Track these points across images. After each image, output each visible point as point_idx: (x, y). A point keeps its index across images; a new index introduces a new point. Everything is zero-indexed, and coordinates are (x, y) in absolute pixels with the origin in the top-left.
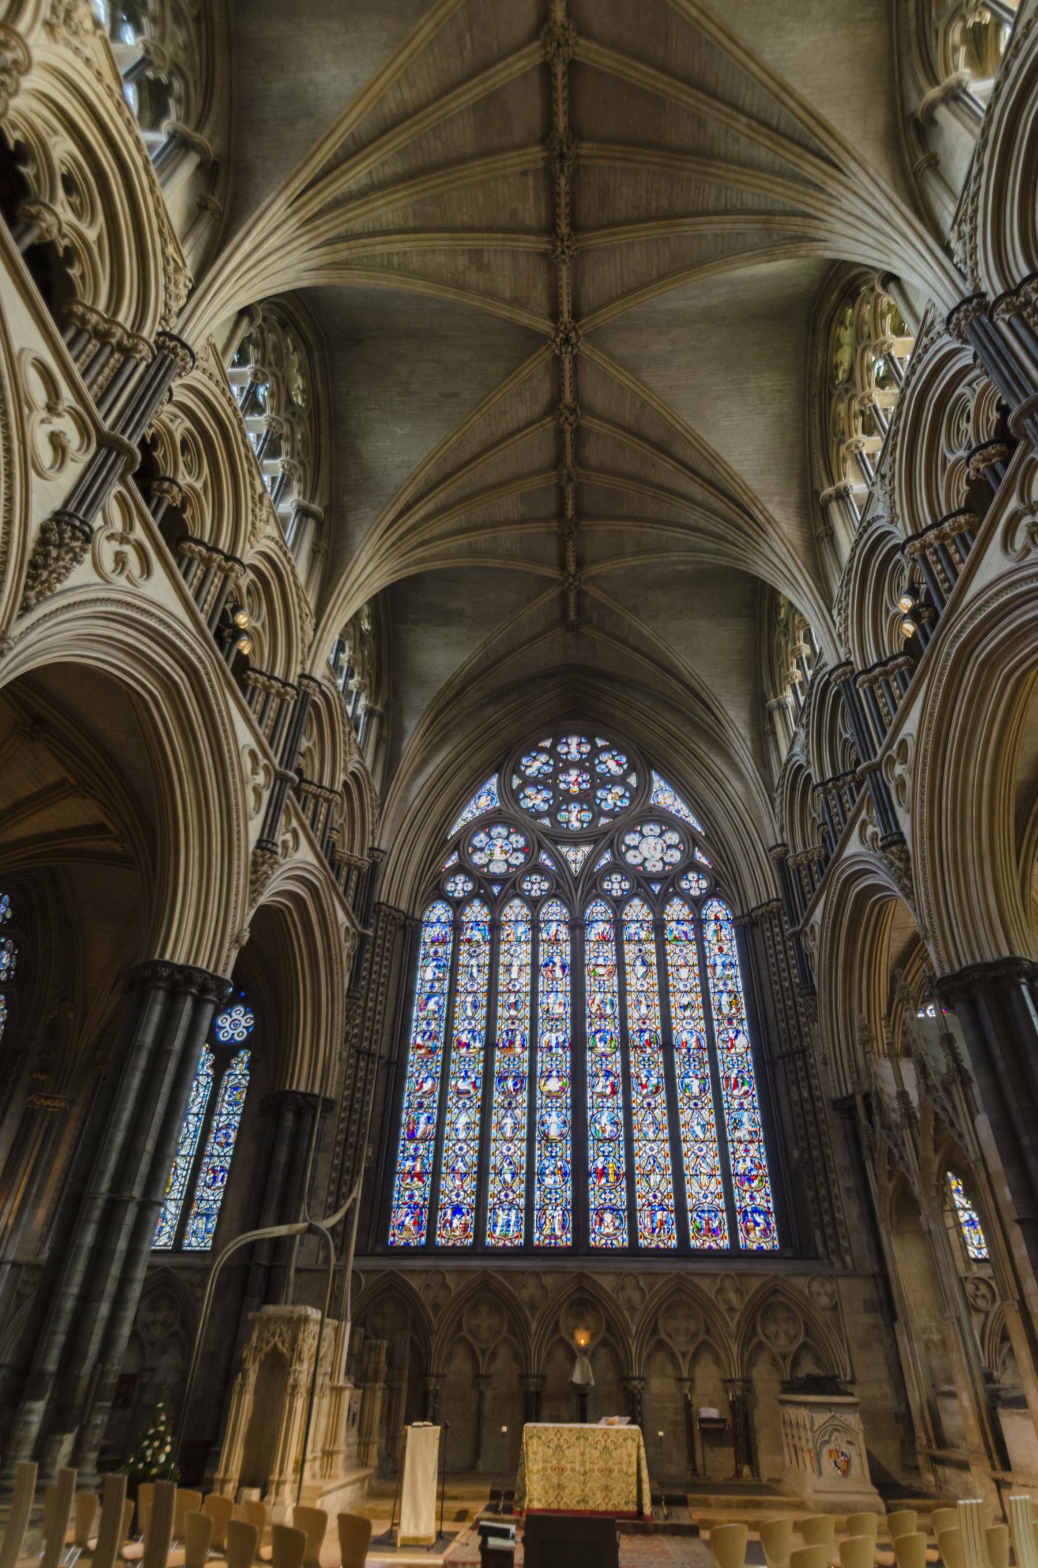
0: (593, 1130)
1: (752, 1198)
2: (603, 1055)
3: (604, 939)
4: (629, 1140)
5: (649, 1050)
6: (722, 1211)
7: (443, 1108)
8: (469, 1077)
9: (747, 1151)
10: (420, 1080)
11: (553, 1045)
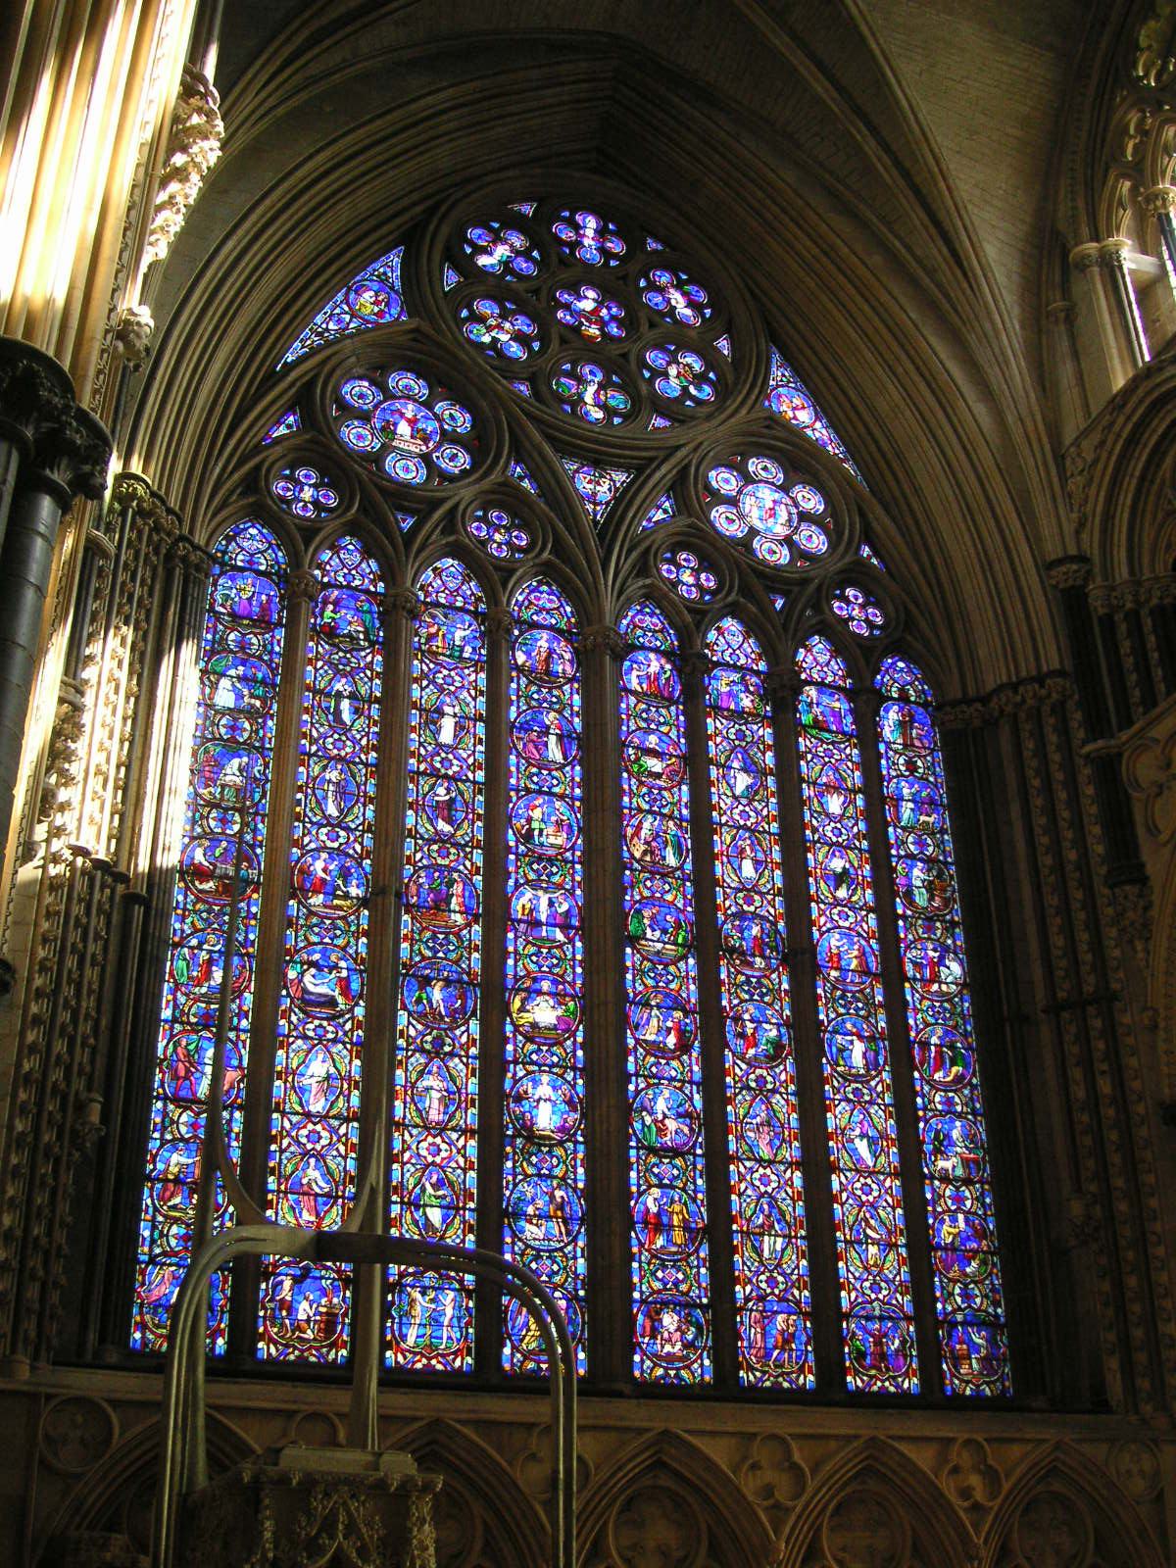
0: (637, 1126)
1: (967, 1296)
2: (658, 958)
3: (657, 695)
4: (718, 1163)
5: (759, 962)
6: (908, 1319)
7: (265, 1040)
8: (336, 967)
9: (959, 1199)
10: (204, 956)
11: (543, 918)
